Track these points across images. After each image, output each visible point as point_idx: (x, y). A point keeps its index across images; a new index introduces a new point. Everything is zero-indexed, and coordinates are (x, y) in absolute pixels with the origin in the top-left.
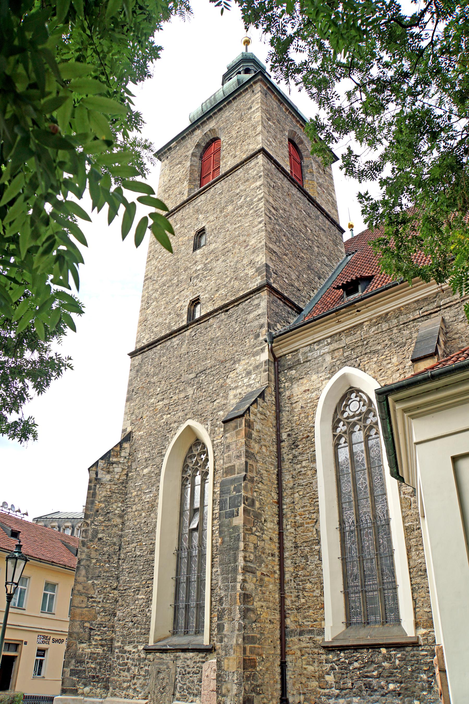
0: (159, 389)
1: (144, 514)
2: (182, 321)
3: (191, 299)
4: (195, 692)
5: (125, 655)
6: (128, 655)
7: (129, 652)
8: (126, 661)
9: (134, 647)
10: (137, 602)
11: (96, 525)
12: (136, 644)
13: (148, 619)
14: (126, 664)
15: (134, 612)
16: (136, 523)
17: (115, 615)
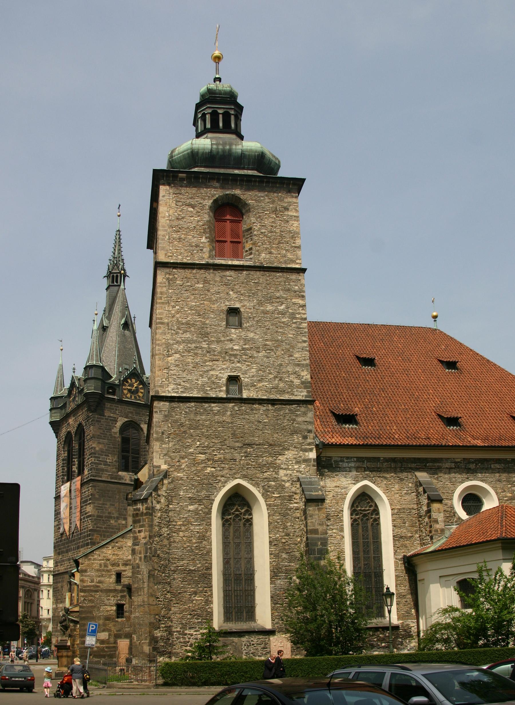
0: (198, 443)
1: (194, 541)
2: (220, 391)
3: (229, 374)
4: (260, 654)
5: (186, 636)
6: (189, 636)
7: (192, 635)
8: (187, 640)
9: (196, 631)
10: (194, 602)
11: (155, 544)
12: (197, 629)
13: (211, 614)
14: (188, 642)
15: (193, 609)
16: (185, 546)
17: (170, 610)
